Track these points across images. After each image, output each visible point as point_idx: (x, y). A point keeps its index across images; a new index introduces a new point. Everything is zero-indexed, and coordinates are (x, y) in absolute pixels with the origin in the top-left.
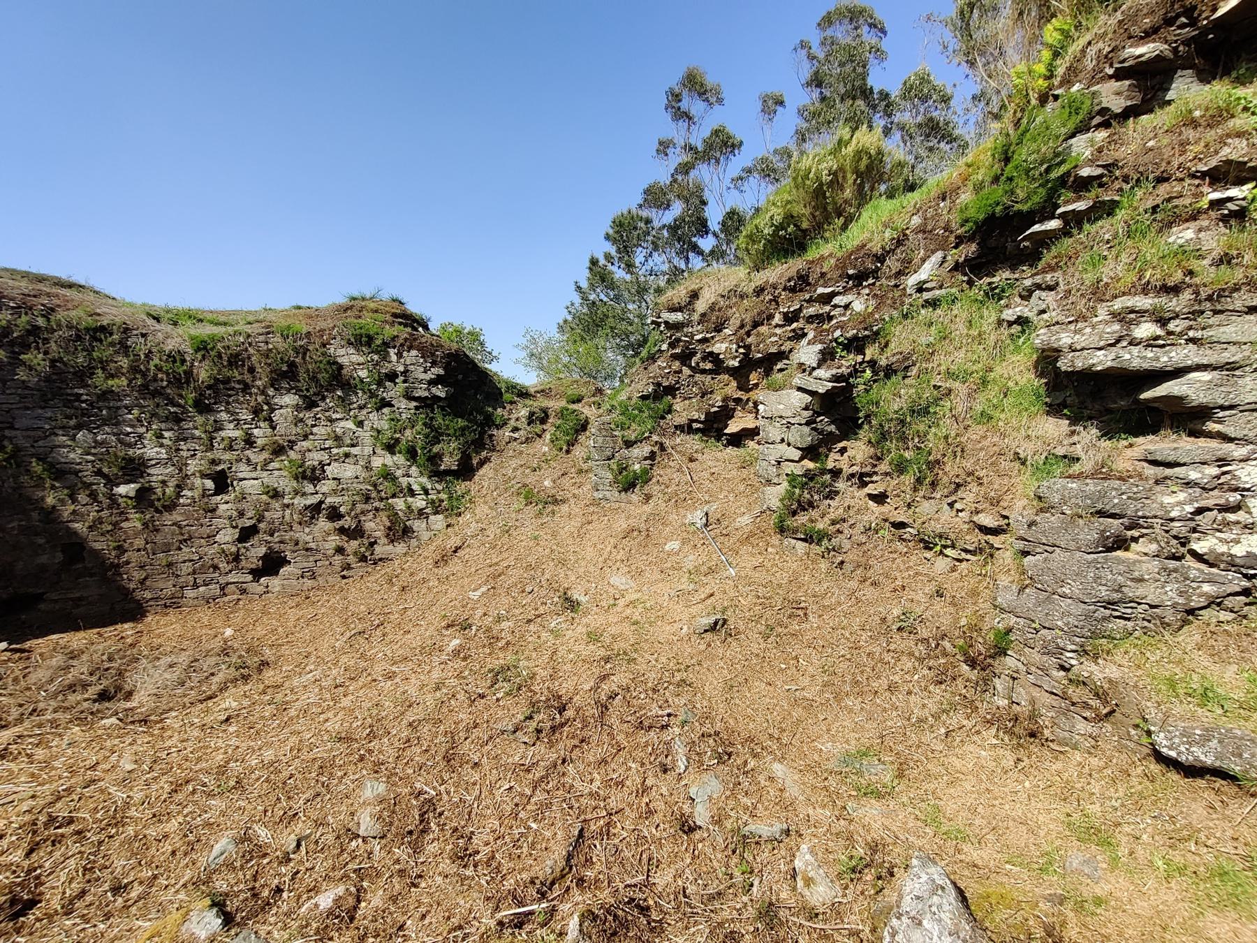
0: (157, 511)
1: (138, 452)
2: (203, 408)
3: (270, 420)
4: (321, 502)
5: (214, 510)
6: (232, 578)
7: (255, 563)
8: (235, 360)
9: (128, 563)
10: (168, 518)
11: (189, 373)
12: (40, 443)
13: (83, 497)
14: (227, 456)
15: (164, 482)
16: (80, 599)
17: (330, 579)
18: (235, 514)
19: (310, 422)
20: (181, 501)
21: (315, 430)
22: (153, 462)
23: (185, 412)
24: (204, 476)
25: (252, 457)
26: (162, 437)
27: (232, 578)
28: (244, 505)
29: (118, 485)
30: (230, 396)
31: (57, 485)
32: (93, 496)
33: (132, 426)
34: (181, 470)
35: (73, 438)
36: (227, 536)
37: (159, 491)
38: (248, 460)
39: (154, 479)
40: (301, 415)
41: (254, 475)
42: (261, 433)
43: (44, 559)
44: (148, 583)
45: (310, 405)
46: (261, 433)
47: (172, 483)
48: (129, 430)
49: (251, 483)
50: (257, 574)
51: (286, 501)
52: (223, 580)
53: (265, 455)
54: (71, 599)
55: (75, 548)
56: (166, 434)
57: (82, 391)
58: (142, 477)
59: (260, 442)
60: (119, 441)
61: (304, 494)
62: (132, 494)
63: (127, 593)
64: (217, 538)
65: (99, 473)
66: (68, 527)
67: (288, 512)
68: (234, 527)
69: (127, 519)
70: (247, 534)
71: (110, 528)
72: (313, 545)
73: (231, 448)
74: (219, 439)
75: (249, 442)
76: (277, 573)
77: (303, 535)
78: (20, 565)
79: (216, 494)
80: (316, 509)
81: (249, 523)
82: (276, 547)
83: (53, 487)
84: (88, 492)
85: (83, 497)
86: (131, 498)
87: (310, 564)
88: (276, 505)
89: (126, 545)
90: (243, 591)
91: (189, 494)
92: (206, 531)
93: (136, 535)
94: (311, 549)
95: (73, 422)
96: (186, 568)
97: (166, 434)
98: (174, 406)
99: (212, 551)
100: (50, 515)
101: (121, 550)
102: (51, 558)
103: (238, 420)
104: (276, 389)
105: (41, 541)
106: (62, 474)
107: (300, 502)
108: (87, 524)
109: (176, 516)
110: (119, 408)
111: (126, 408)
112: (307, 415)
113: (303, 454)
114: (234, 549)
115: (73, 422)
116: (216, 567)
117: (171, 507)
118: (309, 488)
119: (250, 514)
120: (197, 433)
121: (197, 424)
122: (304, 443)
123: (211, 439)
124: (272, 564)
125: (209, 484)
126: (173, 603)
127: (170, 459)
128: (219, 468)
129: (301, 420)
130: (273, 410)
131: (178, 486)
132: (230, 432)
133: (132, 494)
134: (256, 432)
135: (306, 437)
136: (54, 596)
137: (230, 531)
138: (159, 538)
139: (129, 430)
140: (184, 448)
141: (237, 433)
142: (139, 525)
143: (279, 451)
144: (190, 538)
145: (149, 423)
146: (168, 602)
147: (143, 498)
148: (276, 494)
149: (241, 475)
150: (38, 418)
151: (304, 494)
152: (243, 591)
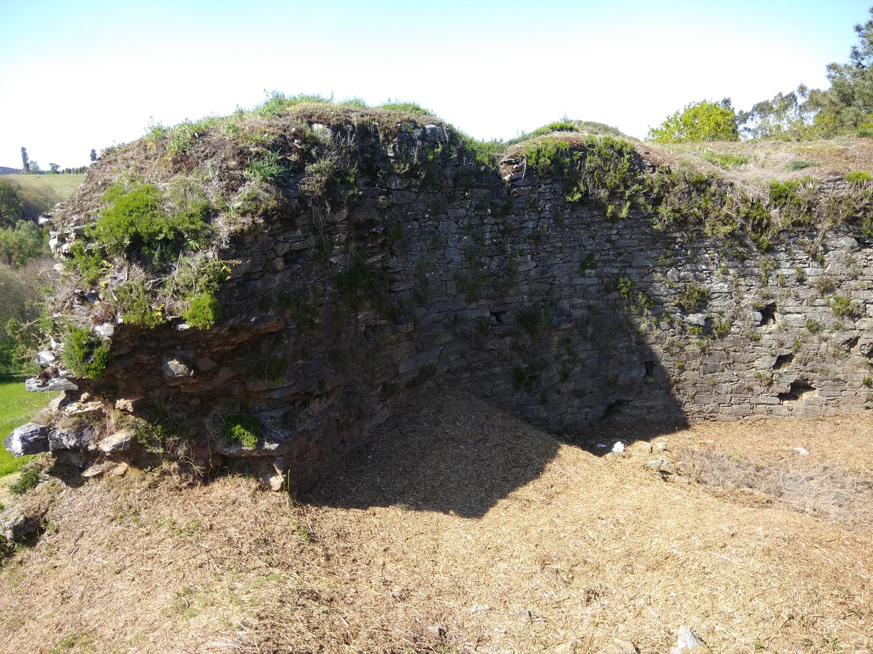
0: (714, 338)
1: (708, 286)
2: (770, 250)
3: (822, 262)
4: (858, 338)
5: (757, 340)
6: (761, 399)
7: (785, 388)
8: (811, 206)
9: (685, 380)
10: (718, 346)
11: (769, 219)
12: (645, 279)
13: (664, 324)
14: (777, 292)
15: (721, 314)
16: (651, 408)
17: (854, 408)
18: (775, 343)
19: (863, 264)
20: (732, 330)
21: (865, 271)
22: (716, 295)
23: (750, 251)
24: (756, 308)
25: (802, 295)
26: (727, 273)
27: (761, 399)
28: (783, 336)
29: (687, 314)
30: (790, 237)
31: (650, 313)
32: (671, 324)
33: (707, 264)
34: (738, 303)
35: (665, 274)
36: (764, 363)
37: (716, 320)
38: (797, 296)
39: (715, 309)
40: (854, 256)
41: (799, 309)
42: (812, 272)
43: (634, 373)
44: (696, 398)
45: (862, 244)
46: (812, 272)
47: (728, 314)
48: (704, 267)
49: (793, 315)
50: (782, 396)
51: (825, 334)
52: (753, 400)
53: (814, 292)
54: (647, 407)
55: (651, 364)
56: (731, 271)
57: (678, 235)
58: (706, 308)
59: (810, 280)
60: (696, 277)
61: (845, 330)
62: (702, 323)
63: (679, 405)
64: (756, 363)
65: (680, 306)
66: (651, 350)
67: (824, 344)
68: (773, 355)
69: (689, 344)
70: (782, 360)
71: (678, 350)
72: (842, 377)
73: (783, 285)
74: (774, 276)
75: (801, 281)
76: (796, 398)
77: (838, 369)
78: (621, 378)
79: (761, 325)
80: (852, 342)
81: (786, 352)
82: (806, 375)
83: (647, 316)
84: (669, 320)
85: (664, 324)
86: (700, 326)
87: (836, 393)
88: (815, 338)
89: (686, 365)
90: (771, 412)
91: (740, 324)
92: (749, 356)
93: (695, 356)
94: (838, 380)
95: (668, 261)
96: (727, 387)
97: (731, 271)
98: (742, 247)
99: (750, 374)
100: (641, 339)
101: (682, 369)
102: (637, 373)
103: (794, 260)
104: (836, 232)
105: (635, 359)
106: (656, 305)
107: (838, 337)
108: (664, 346)
109: (727, 342)
110: (700, 248)
111: (705, 248)
112: (859, 256)
113: (849, 291)
114: (769, 375)
115: (668, 261)
116: (750, 389)
117: (722, 336)
118: (848, 323)
119: (788, 345)
120: (756, 270)
121: (758, 262)
122: (853, 283)
123: (768, 276)
124: (798, 388)
125: (759, 316)
126: (711, 417)
127: (731, 293)
128: (770, 302)
129: (854, 261)
130: (826, 251)
131: (733, 317)
132: (786, 270)
133: (702, 323)
134: (808, 270)
135: (855, 278)
136: (637, 403)
137: (768, 358)
138: (708, 361)
139: (704, 267)
140: (743, 283)
141: (793, 271)
142: (698, 350)
143: (827, 289)
144: (734, 362)
145: (719, 262)
146: (708, 415)
147: (707, 329)
148: (814, 328)
149: (787, 309)
150: (647, 258)
151: (845, 330)
152: (771, 412)
